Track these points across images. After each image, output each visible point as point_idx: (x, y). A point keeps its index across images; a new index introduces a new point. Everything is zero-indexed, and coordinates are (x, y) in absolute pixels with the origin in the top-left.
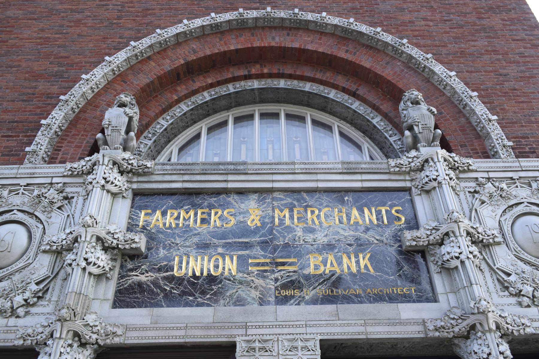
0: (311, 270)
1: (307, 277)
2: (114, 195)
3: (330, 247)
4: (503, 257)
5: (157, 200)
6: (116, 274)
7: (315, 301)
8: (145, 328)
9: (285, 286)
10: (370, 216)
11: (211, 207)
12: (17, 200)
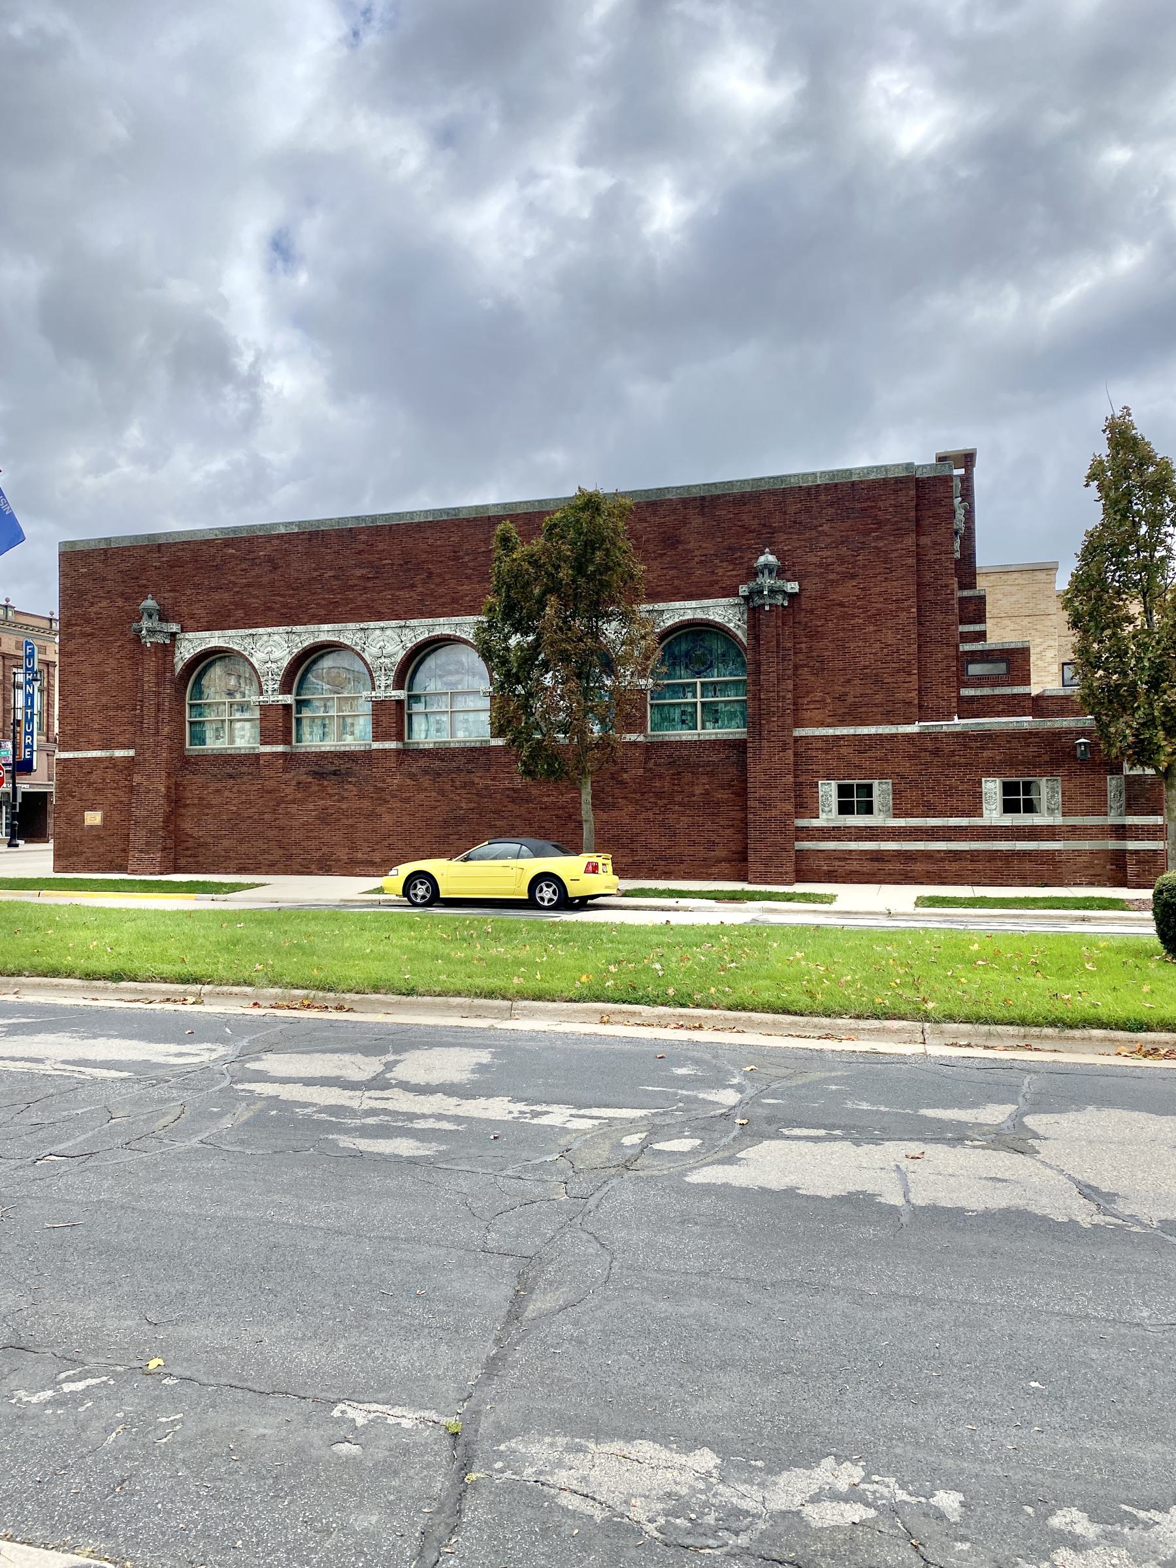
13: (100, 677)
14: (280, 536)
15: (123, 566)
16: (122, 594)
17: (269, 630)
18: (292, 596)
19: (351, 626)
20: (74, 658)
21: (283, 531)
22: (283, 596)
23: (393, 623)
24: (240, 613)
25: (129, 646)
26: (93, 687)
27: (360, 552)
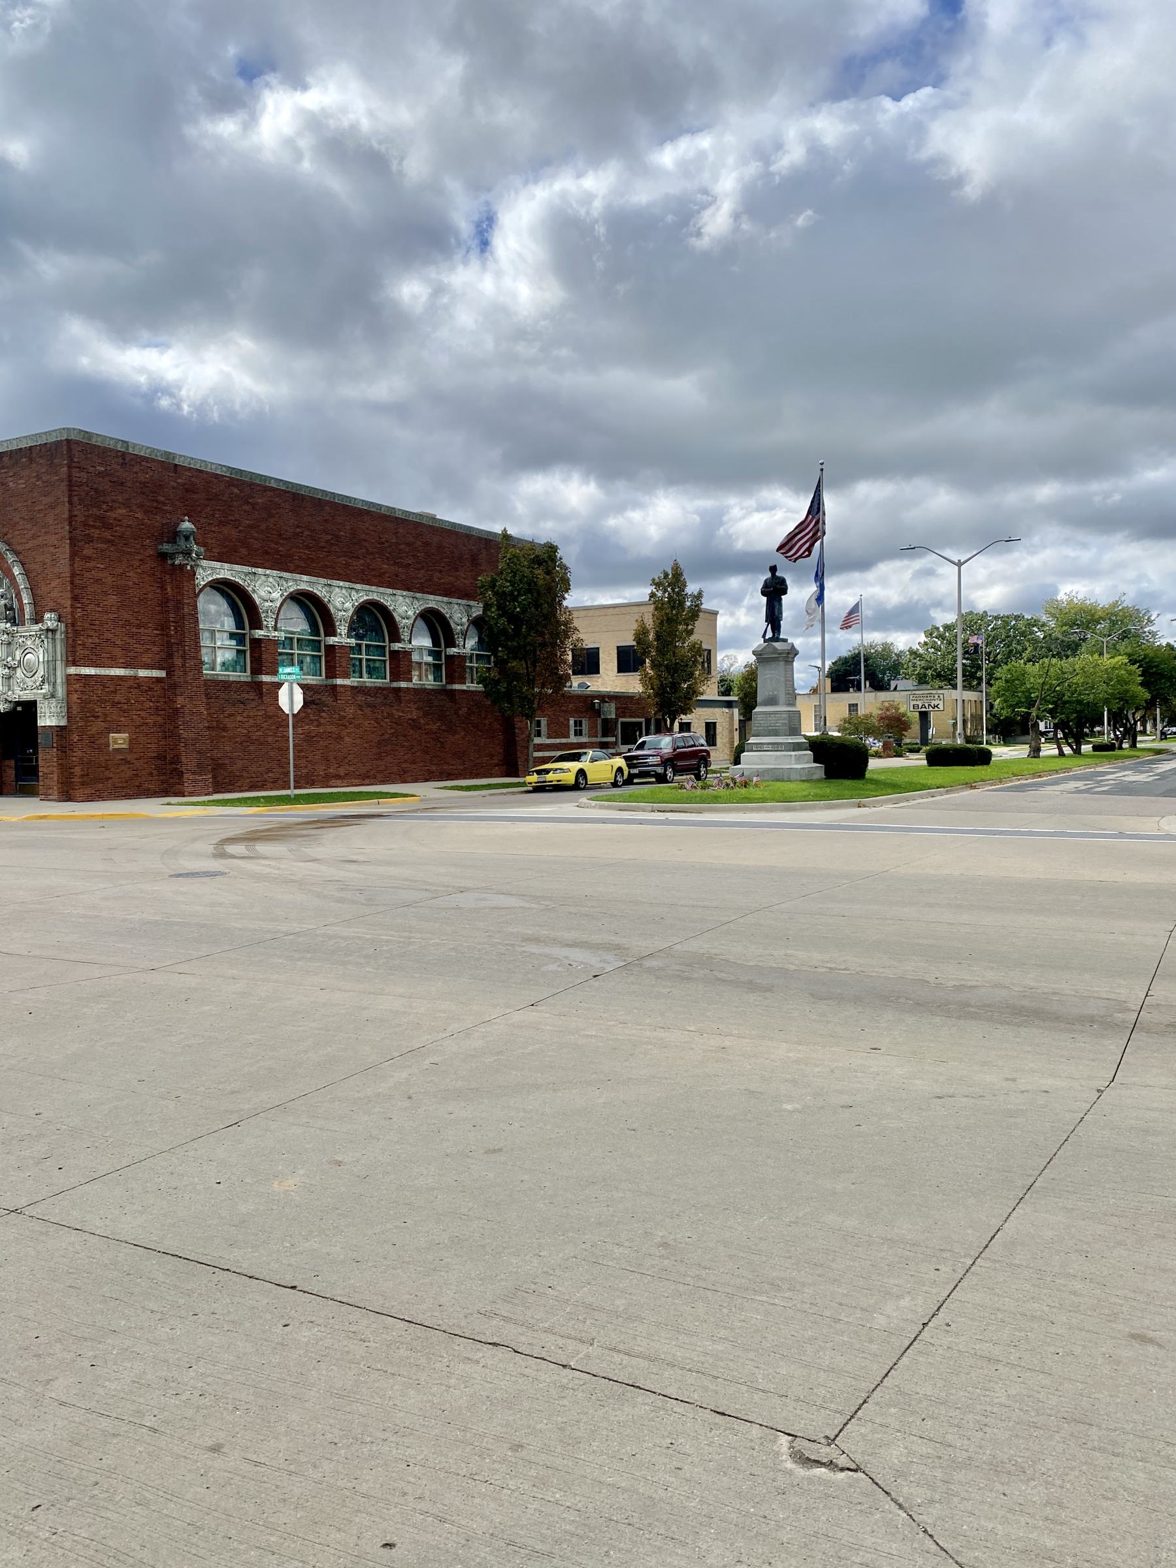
13: (121, 590)
14: (273, 489)
15: (142, 477)
17: (268, 572)
18: (282, 545)
19: (322, 581)
20: (92, 564)
21: (273, 484)
23: (347, 584)
24: (244, 551)
26: (113, 599)
27: (326, 521)
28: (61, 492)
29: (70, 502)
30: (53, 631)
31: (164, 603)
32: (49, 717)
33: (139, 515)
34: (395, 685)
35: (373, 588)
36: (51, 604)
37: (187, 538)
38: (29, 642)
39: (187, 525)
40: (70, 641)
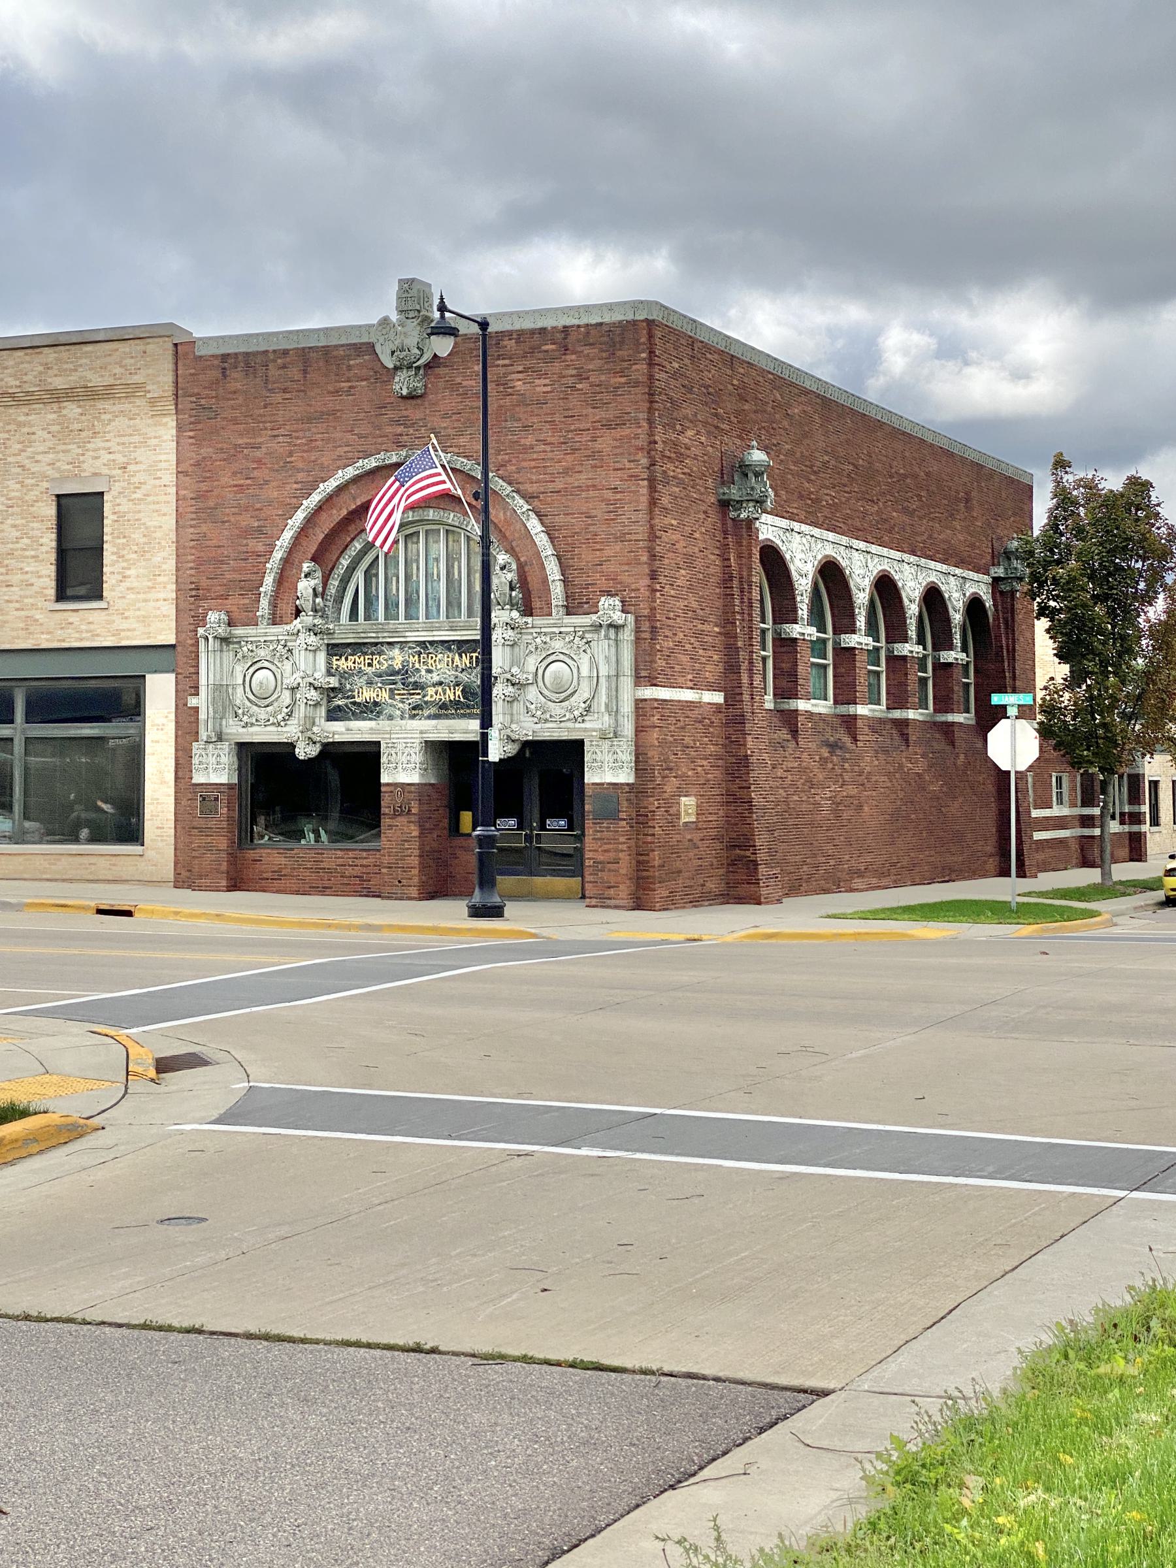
0: (427, 698)
1: (426, 703)
2: (315, 651)
3: (441, 683)
4: (532, 693)
5: (342, 650)
6: (324, 702)
7: (429, 717)
8: (342, 734)
9: (414, 708)
10: (466, 660)
11: (373, 654)
12: (262, 653)
16: (705, 423)
19: (844, 540)
20: (667, 521)
22: (809, 481)
25: (714, 517)
28: (633, 403)
29: (650, 422)
30: (617, 627)
31: (727, 580)
32: (607, 768)
33: (703, 439)
34: (897, 714)
35: (885, 551)
36: (603, 584)
37: (757, 475)
38: (558, 645)
39: (758, 456)
40: (645, 645)
